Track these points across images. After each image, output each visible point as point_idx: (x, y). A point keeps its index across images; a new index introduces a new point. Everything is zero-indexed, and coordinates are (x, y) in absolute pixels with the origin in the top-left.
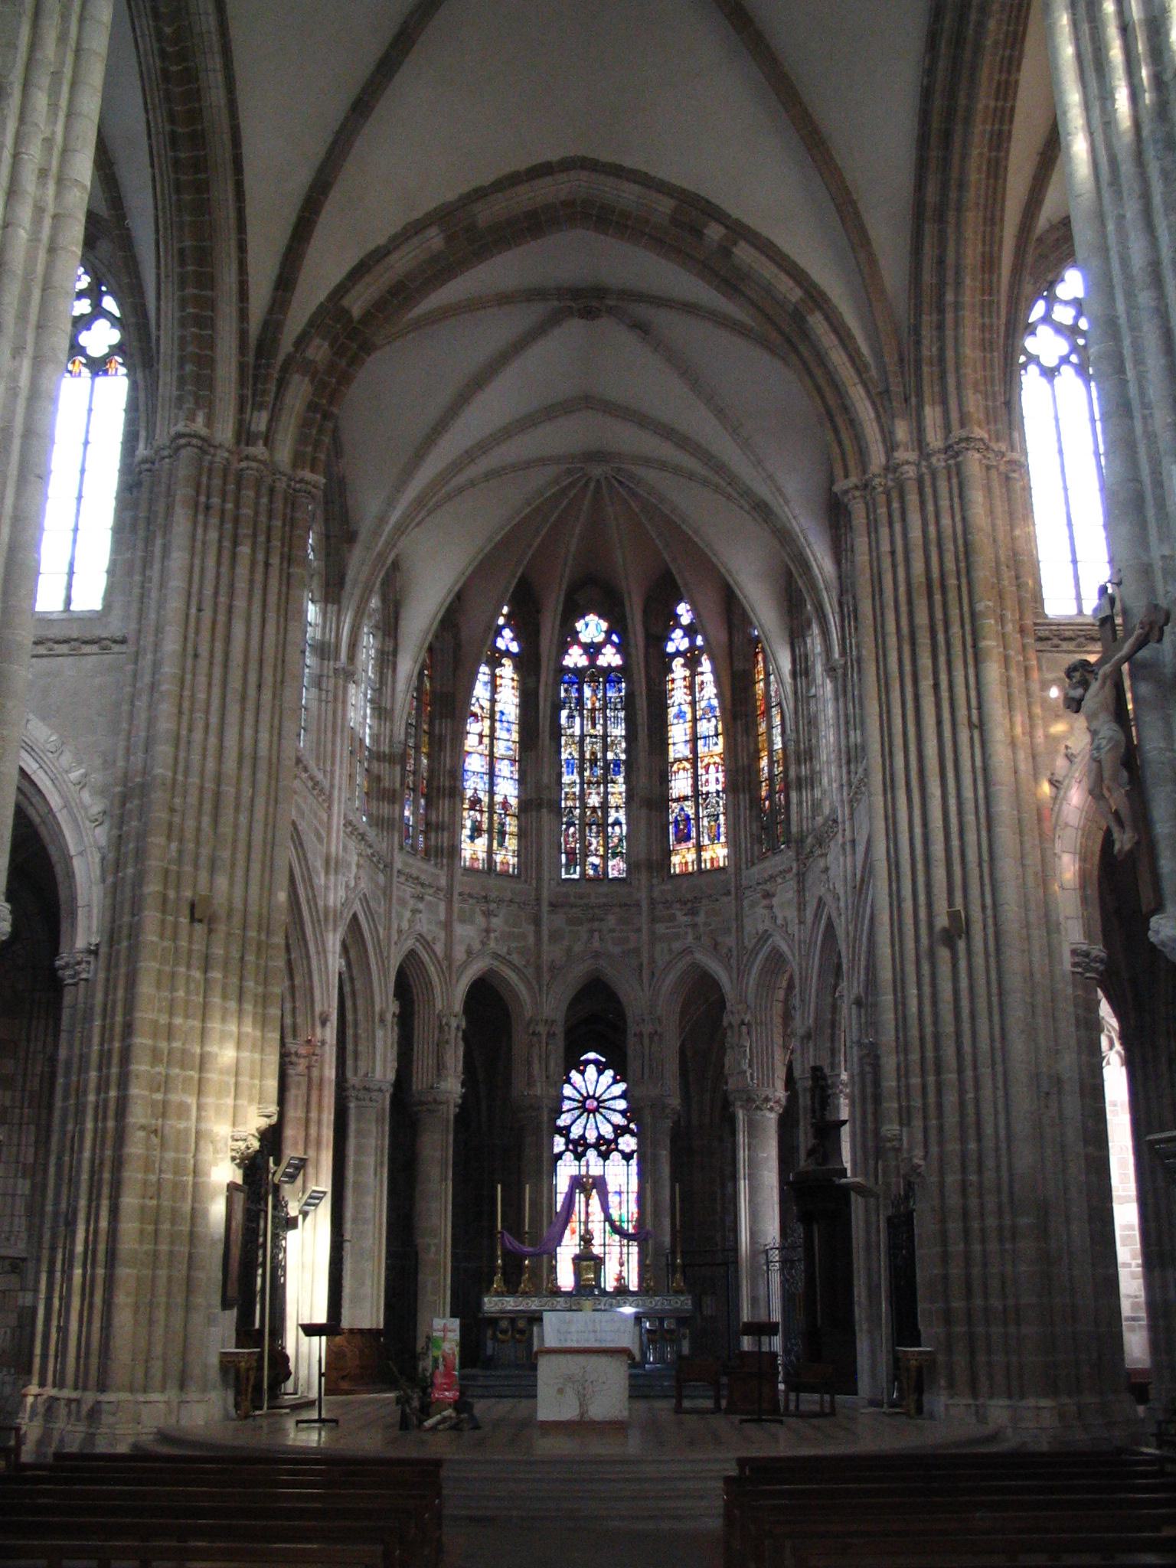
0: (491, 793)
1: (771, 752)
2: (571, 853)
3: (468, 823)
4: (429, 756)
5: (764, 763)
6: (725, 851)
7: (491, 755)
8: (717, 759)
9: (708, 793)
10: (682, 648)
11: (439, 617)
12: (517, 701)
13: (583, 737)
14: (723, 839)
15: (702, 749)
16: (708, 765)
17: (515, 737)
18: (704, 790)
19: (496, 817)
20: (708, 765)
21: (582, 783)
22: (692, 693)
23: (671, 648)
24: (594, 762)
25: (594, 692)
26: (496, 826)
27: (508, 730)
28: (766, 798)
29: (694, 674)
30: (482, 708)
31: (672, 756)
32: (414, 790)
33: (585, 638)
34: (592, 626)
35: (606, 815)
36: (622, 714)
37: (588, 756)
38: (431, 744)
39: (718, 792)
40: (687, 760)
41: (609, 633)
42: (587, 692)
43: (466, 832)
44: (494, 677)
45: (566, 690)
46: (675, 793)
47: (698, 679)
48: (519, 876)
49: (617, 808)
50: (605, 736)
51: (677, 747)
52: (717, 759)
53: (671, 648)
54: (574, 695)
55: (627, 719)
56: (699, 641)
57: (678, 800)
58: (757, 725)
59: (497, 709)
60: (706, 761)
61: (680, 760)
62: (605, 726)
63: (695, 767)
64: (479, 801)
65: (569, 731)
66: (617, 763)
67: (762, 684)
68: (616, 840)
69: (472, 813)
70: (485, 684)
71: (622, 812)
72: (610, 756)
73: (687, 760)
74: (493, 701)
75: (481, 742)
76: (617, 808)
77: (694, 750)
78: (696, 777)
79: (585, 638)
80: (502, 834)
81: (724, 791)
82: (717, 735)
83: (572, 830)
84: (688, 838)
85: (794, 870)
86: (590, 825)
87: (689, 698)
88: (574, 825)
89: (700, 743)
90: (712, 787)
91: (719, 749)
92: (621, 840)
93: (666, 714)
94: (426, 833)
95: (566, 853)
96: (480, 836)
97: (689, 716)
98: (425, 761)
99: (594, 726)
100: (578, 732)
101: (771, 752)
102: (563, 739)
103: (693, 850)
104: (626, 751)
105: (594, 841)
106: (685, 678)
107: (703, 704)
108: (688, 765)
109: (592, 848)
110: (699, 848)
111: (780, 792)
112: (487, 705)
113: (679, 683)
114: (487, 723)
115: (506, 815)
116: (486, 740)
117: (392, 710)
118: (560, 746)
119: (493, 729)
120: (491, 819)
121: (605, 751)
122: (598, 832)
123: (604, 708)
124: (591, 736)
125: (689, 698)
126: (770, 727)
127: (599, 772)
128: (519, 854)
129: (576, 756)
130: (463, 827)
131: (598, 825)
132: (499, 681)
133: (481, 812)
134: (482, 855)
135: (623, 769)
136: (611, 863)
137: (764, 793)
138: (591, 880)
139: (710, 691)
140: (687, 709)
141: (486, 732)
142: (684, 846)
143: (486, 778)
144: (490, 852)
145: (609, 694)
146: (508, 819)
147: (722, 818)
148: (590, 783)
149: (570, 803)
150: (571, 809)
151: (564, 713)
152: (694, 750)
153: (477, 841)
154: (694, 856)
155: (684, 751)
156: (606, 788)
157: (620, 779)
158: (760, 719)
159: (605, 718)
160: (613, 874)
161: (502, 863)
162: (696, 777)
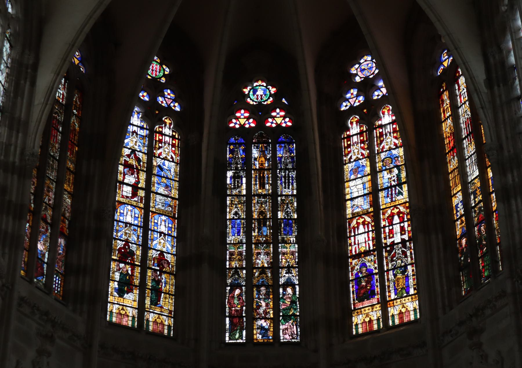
0: (145, 247)
1: (465, 184)
2: (236, 317)
3: (117, 276)
4: (72, 196)
5: (457, 200)
6: (416, 304)
7: (147, 209)
8: (402, 209)
9: (393, 243)
10: (357, 104)
11: (87, 29)
12: (177, 159)
13: (249, 195)
14: (412, 291)
15: (383, 199)
16: (392, 215)
17: (175, 193)
18: (389, 241)
19: (149, 273)
20: (392, 215)
21: (249, 243)
22: (371, 147)
23: (344, 107)
24: (262, 222)
25: (263, 153)
26: (150, 284)
27: (167, 186)
28: (462, 237)
29: (371, 128)
30: (138, 160)
31: (349, 211)
32: (51, 225)
33: (252, 100)
34: (260, 92)
35: (276, 276)
36: (293, 174)
37: (255, 216)
38: (76, 184)
39: (403, 242)
40: (367, 213)
41: (276, 96)
42: (255, 153)
43: (114, 285)
44: (152, 132)
45: (232, 152)
46: (353, 250)
47: (376, 133)
48: (174, 339)
49: (289, 269)
50: (274, 195)
51: (356, 202)
52: (402, 209)
53: (344, 107)
54: (241, 154)
55: (298, 179)
56: (377, 95)
57: (358, 256)
58: (445, 164)
59: (156, 162)
60: (389, 212)
61: (359, 215)
62: (274, 186)
63: (376, 219)
64: (132, 254)
65: (234, 192)
66: (288, 221)
67: (449, 121)
68: (288, 302)
69: (122, 265)
70: (143, 137)
71: (294, 272)
72: (280, 215)
73: (367, 213)
74: (151, 155)
75: (134, 194)
76: (289, 269)
77: (375, 203)
78: (378, 229)
79: (252, 100)
80: (157, 292)
81: (410, 239)
82: (400, 184)
83: (237, 292)
84: (371, 294)
85: (509, 290)
86: (258, 287)
87: (366, 153)
88: (240, 286)
89: (382, 194)
90: (397, 239)
91: (404, 197)
92: (293, 302)
93: (342, 171)
94: (65, 277)
95: (231, 317)
96: (130, 291)
97: (368, 169)
98: (69, 201)
99: (262, 186)
100: (244, 192)
101: (465, 184)
102: (228, 198)
103: (378, 307)
104: (298, 210)
105: (263, 304)
106: (361, 133)
107: (383, 155)
108: (368, 219)
109: (261, 311)
110: (384, 304)
111: (479, 223)
112: (144, 158)
113: (355, 139)
114: (143, 176)
115: (162, 272)
116: (142, 193)
117: (27, 123)
118: (224, 206)
119: (148, 181)
120: (143, 274)
121: (275, 211)
122: (267, 295)
123: (273, 168)
124: (259, 196)
125: (366, 153)
126: (462, 160)
127: (266, 231)
128: (176, 314)
129: (243, 216)
130: (109, 279)
131: (267, 287)
132: (158, 137)
133: (133, 266)
134: (131, 312)
135: (295, 228)
136: (282, 327)
137: (459, 233)
138: (259, 344)
139: (390, 141)
140: (366, 162)
141: (142, 184)
142: (366, 303)
143: (140, 231)
144: (141, 309)
145: (279, 155)
146: (164, 276)
147: (410, 268)
148: (258, 244)
149: (234, 264)
150: (236, 270)
151: (230, 174)
152: (375, 203)
153: (126, 295)
154: (379, 313)
155: (363, 204)
156: (276, 248)
157: (293, 239)
158: (449, 157)
159: (275, 178)
160: (285, 337)
161: (155, 322)
162: (378, 229)
